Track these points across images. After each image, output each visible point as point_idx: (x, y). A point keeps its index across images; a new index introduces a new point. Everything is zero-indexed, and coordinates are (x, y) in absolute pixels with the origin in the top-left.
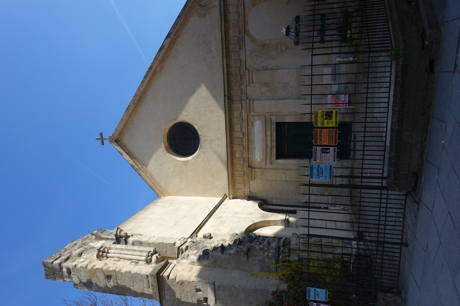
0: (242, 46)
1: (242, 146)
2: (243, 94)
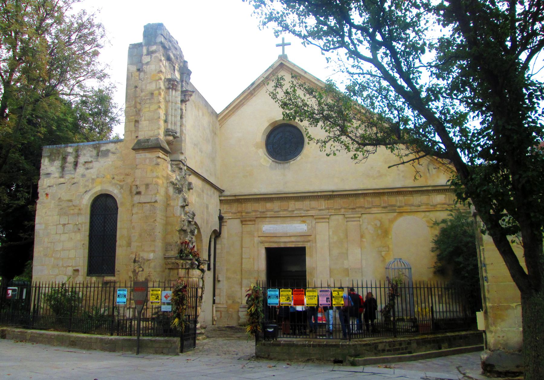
0: (386, 209)
1: (279, 210)
2: (336, 211)
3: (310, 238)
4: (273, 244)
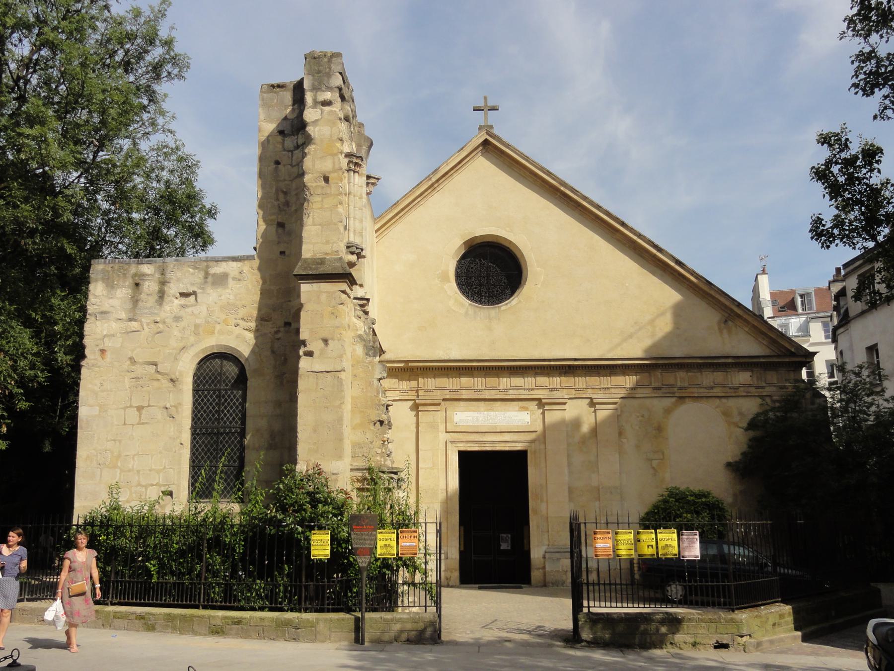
0: (658, 391)
2: (578, 392)
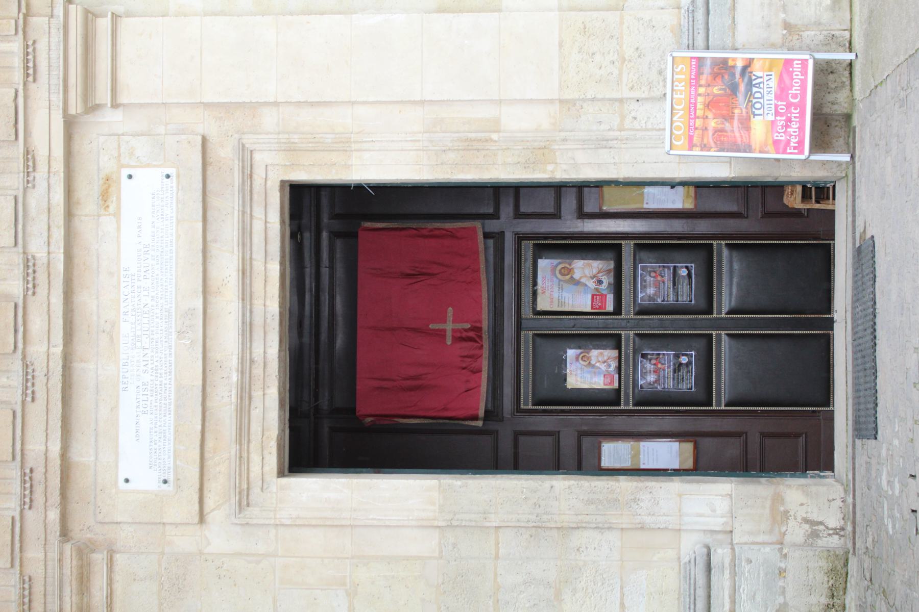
1: (18, 366)
3: (224, 153)
4: (256, 413)
